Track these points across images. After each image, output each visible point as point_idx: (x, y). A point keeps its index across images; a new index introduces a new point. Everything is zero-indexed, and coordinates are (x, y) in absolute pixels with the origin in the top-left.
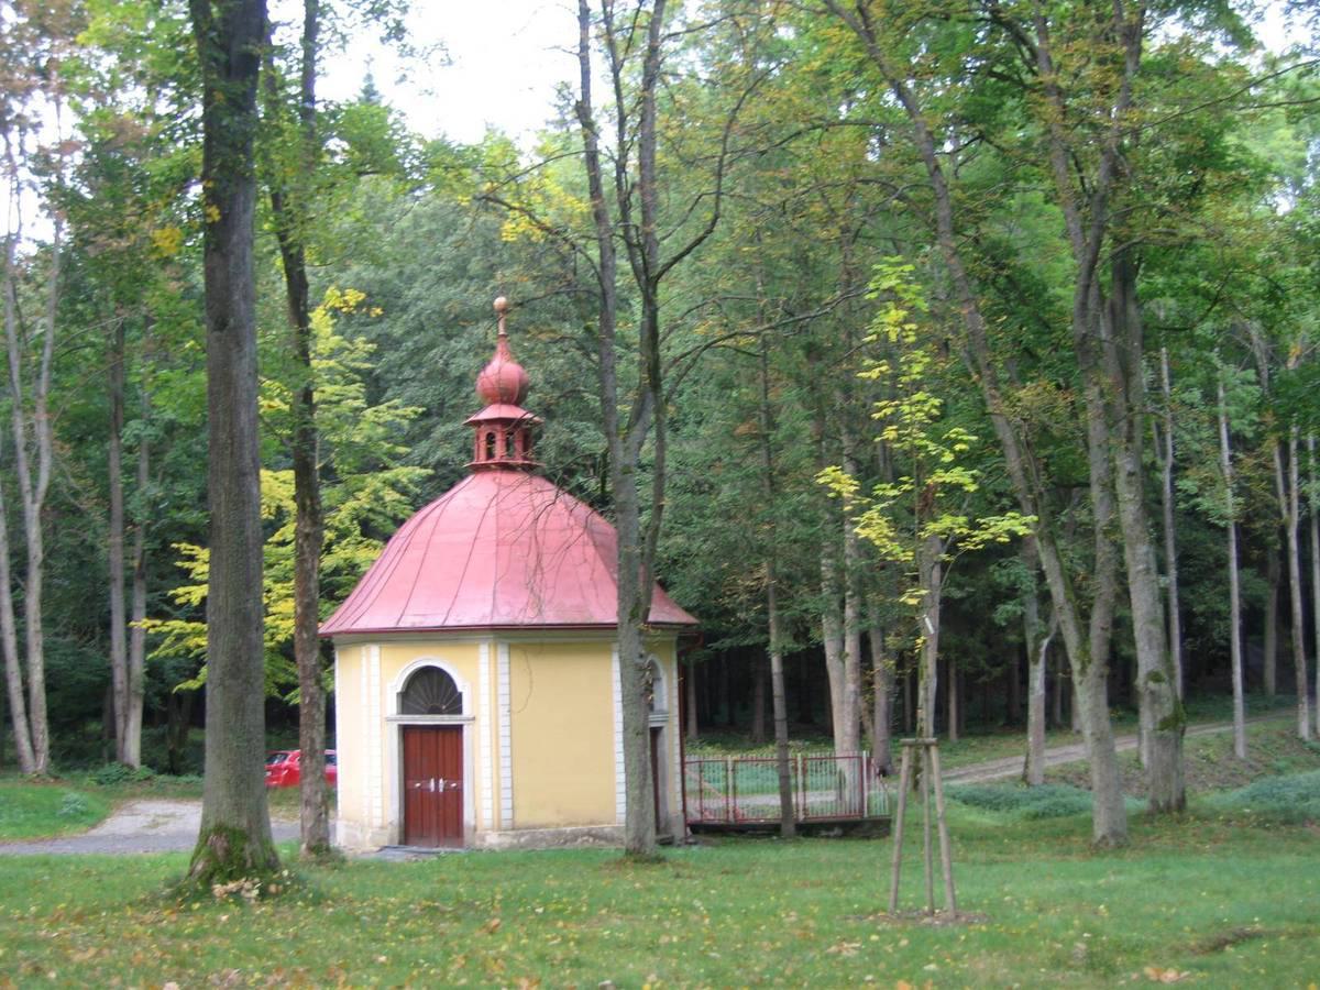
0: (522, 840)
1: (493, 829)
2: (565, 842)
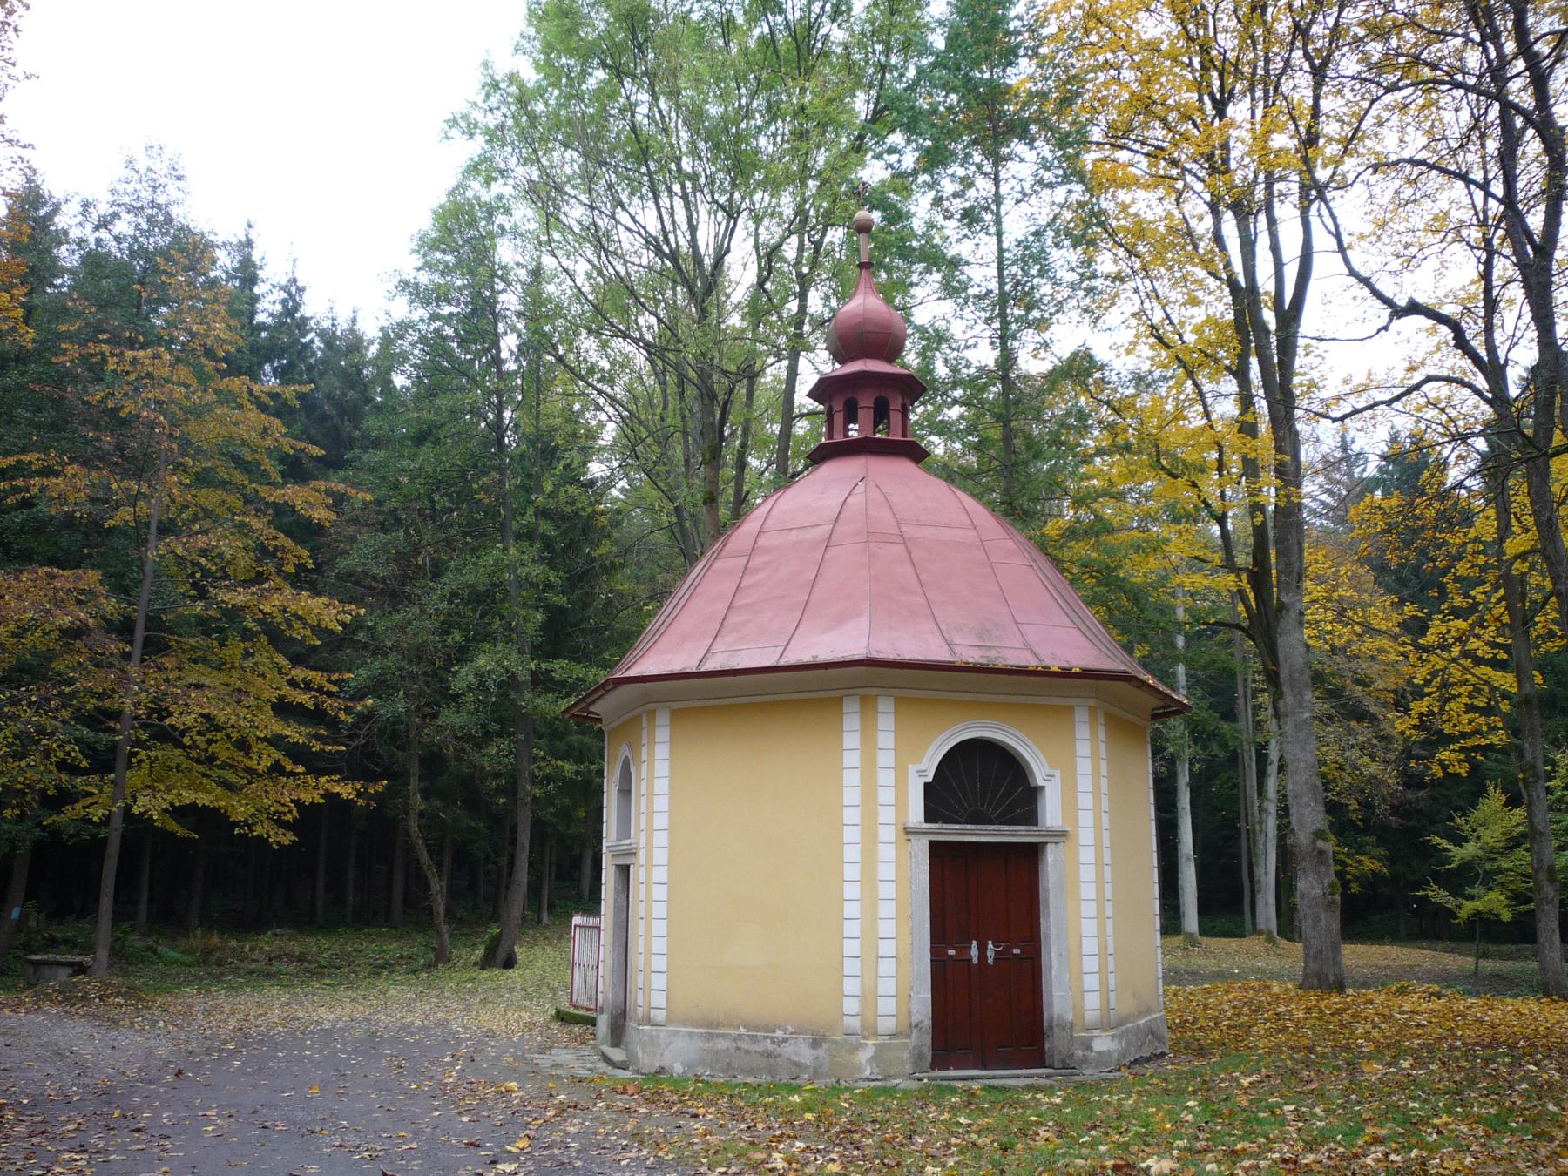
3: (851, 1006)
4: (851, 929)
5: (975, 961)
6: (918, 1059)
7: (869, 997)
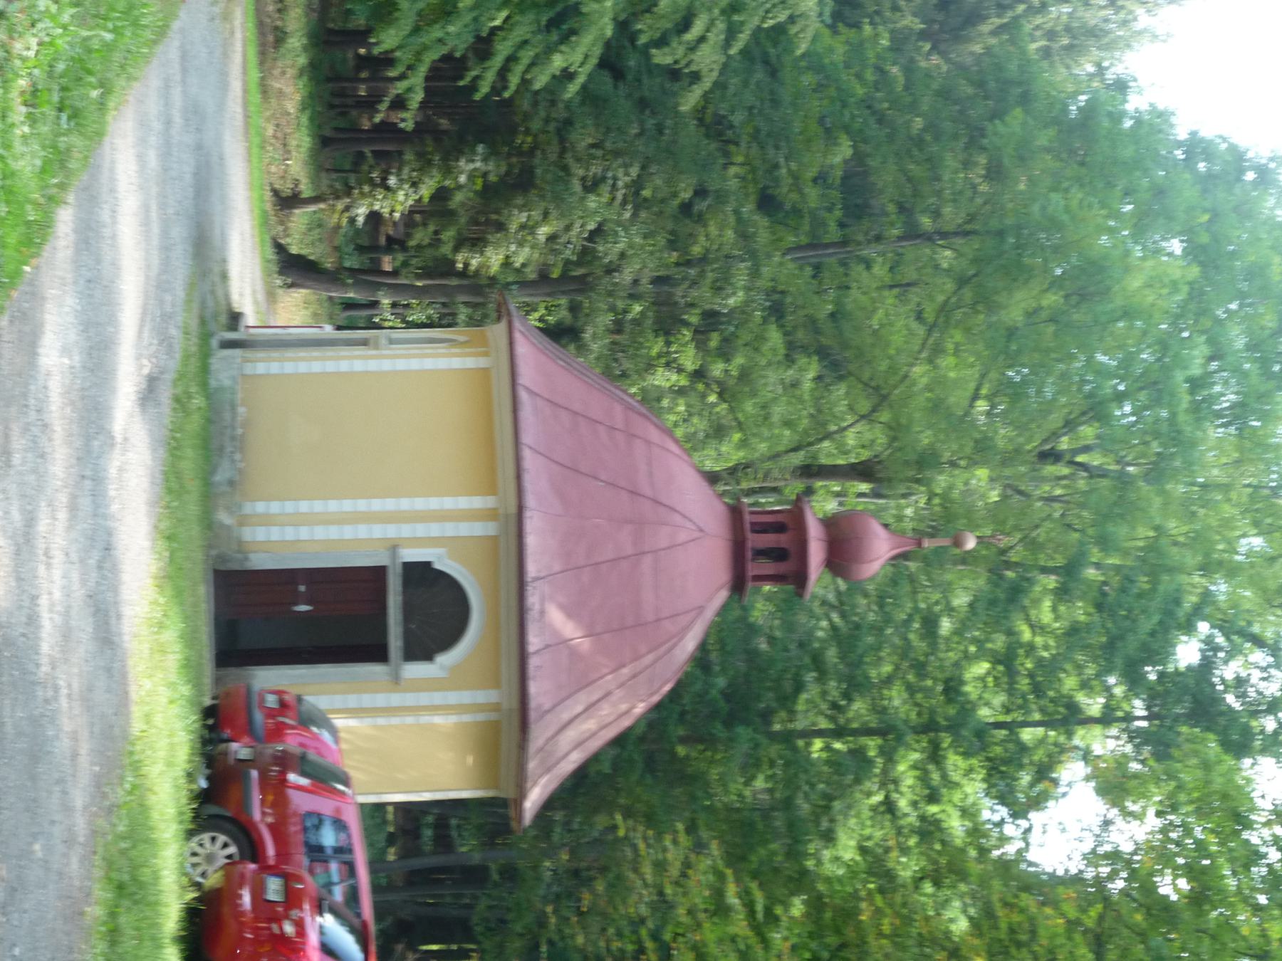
3: (260, 507)
4: (318, 506)
7: (267, 520)
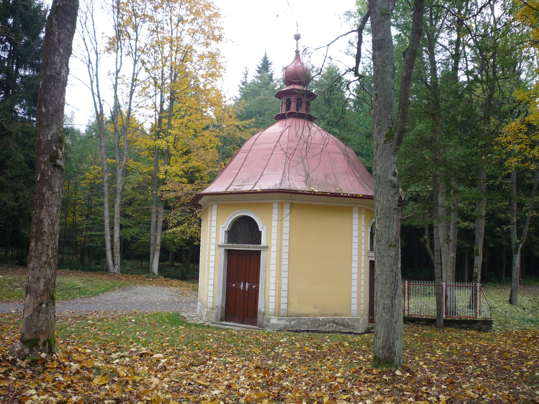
0: (292, 323)
1: (275, 316)
2: (319, 326)
5: (242, 289)
6: (217, 317)
